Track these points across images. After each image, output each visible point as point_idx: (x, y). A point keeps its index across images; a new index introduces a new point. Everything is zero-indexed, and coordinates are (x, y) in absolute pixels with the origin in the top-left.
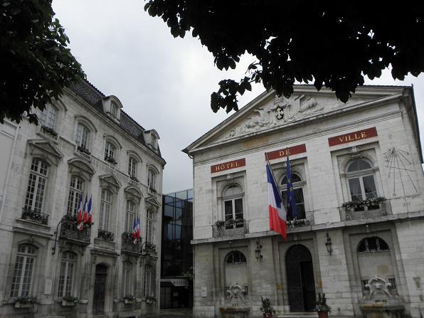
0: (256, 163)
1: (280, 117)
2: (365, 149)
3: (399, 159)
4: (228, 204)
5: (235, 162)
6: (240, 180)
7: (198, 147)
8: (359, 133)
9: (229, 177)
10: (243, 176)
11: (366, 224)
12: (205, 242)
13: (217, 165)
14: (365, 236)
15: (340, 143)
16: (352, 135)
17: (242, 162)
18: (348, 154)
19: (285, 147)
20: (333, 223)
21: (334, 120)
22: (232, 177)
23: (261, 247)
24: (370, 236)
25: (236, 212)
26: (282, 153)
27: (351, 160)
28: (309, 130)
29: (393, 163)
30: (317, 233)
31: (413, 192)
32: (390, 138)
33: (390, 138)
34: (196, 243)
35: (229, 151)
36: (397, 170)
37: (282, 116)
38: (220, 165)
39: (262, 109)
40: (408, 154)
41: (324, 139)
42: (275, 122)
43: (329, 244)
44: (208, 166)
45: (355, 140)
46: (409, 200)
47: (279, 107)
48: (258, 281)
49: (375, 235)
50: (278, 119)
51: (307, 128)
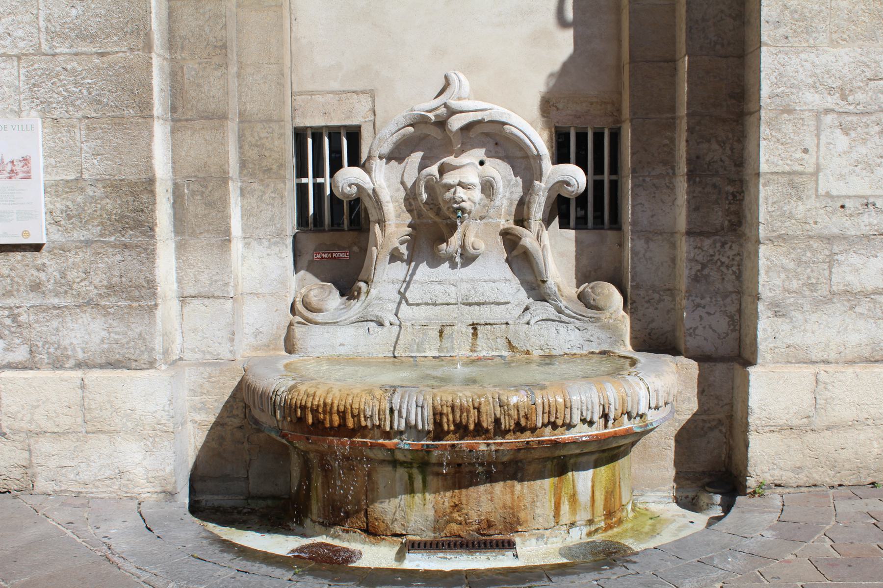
48: (840, 59)
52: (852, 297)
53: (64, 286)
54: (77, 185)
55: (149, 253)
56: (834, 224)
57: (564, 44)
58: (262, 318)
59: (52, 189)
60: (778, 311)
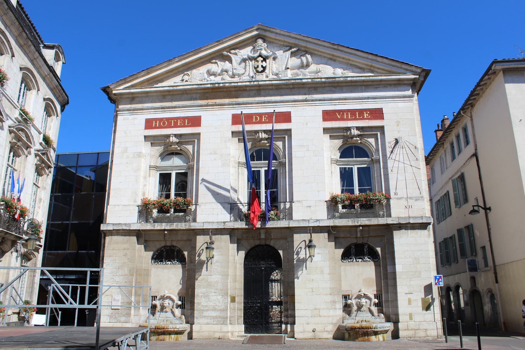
0: (216, 124)
1: (260, 69)
3: (405, 152)
4: (165, 179)
5: (184, 118)
7: (133, 86)
11: (360, 226)
12: (125, 228)
13: (156, 120)
14: (354, 241)
15: (337, 119)
16: (353, 112)
17: (196, 121)
19: (271, 110)
20: (317, 220)
26: (256, 118)
29: (398, 155)
31: (417, 194)
32: (398, 125)
33: (398, 125)
34: (110, 228)
36: (401, 165)
37: (264, 68)
38: (161, 120)
39: (236, 54)
40: (416, 148)
42: (252, 74)
44: (141, 119)
45: (356, 119)
46: (411, 202)
47: (260, 56)
48: (204, 290)
50: (258, 72)
52: (205, 317)
53: (121, 314)
54: (124, 302)
55: (131, 310)
56: (203, 308)
57: (181, 286)
58: (143, 319)
59: (121, 303)
60: (197, 318)
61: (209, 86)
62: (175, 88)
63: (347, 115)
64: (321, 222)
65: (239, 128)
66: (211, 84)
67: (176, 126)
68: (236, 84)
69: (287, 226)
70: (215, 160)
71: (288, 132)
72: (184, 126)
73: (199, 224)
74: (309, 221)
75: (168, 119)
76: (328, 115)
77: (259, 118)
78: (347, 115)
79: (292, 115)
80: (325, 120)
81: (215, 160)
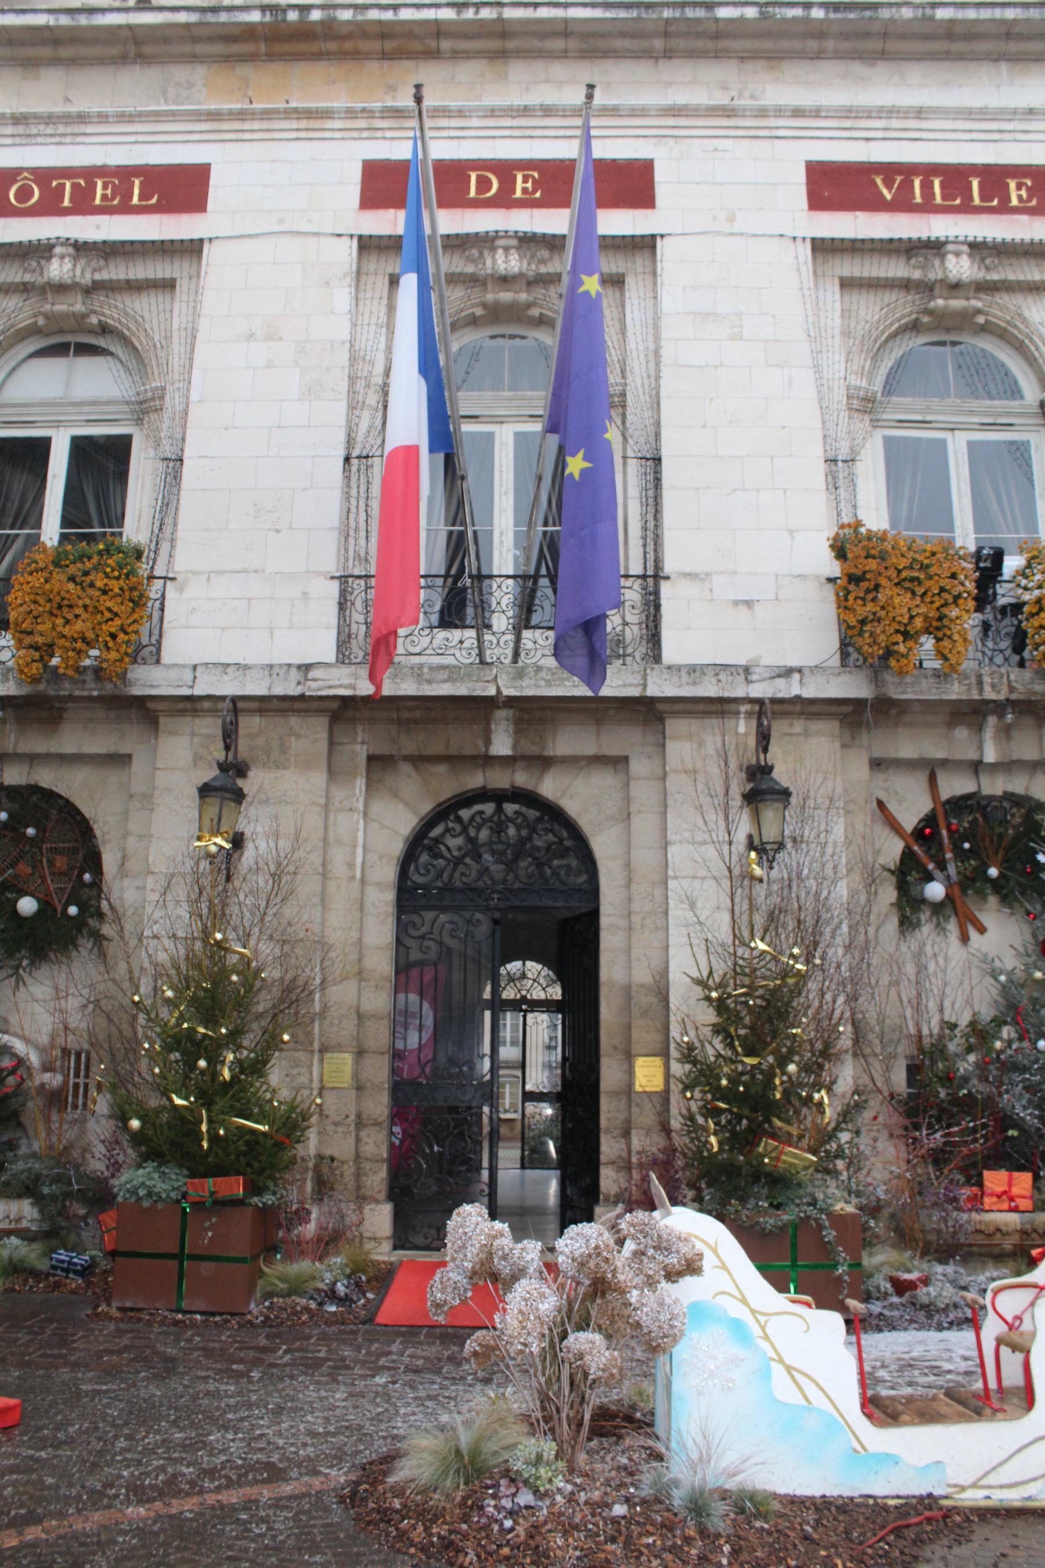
2: (1012, 275)
5: (125, 174)
6: (144, 308)
8: (995, 178)
9: (58, 269)
10: (169, 285)
15: (876, 205)
16: (955, 177)
17: (183, 188)
18: (906, 285)
21: (859, 68)
22: (84, 273)
23: (241, 770)
24: (994, 786)
25: (66, 522)
26: (484, 184)
27: (915, 327)
28: (695, 85)
30: (674, 725)
35: (94, 91)
41: (786, 163)
43: (761, 789)
45: (967, 208)
49: (1018, 785)
51: (678, 71)
61: (255, 17)
62: (83, 20)
63: (927, 187)
64: (809, 679)
65: (389, 222)
66: (264, 8)
67: (83, 205)
68: (389, 15)
69: (635, 692)
70: (270, 365)
71: (645, 245)
72: (126, 208)
73: (173, 674)
74: (747, 670)
75: (44, 175)
76: (833, 185)
77: (501, 182)
78: (927, 187)
79: (660, 175)
80: (817, 201)
81: (270, 365)
